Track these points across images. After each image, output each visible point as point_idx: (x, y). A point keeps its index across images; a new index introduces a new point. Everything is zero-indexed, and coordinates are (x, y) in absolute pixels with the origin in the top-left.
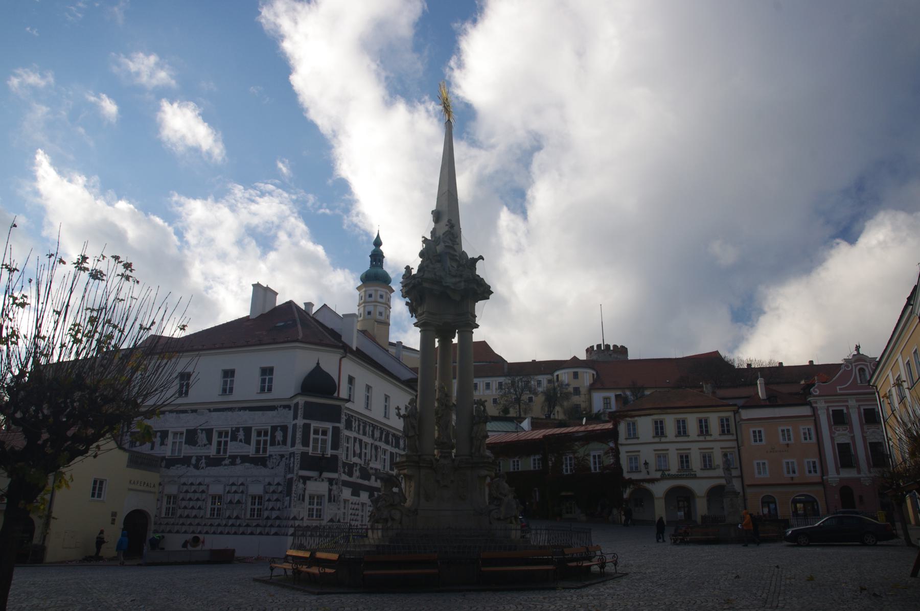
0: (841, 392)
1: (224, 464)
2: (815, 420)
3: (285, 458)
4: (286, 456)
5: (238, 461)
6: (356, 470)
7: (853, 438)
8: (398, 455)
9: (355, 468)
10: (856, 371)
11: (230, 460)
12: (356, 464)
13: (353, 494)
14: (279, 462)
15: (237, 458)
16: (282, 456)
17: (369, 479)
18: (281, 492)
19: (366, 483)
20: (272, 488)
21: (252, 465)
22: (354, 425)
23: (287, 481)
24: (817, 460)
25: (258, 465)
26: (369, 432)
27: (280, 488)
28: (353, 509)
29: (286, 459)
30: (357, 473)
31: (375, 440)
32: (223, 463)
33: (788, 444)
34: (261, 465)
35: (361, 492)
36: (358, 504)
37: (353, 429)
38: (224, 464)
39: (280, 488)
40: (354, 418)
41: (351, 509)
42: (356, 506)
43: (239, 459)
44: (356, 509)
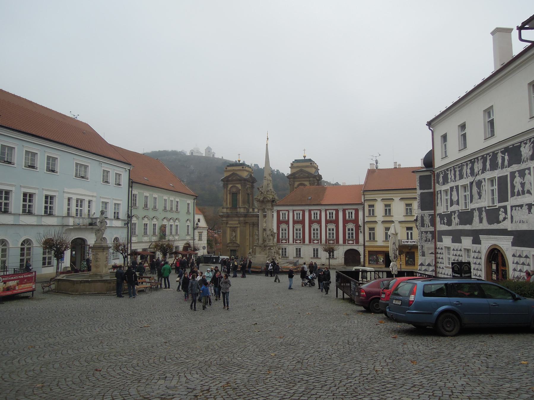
6: (454, 218)
8: (517, 174)
9: (453, 216)
12: (454, 212)
13: (454, 241)
17: (470, 222)
19: (468, 227)
22: (449, 176)
26: (467, 172)
28: (456, 255)
30: (456, 220)
31: (476, 176)
35: (462, 238)
36: (461, 250)
37: (449, 180)
40: (449, 169)
41: (453, 255)
42: (459, 253)
44: (459, 256)
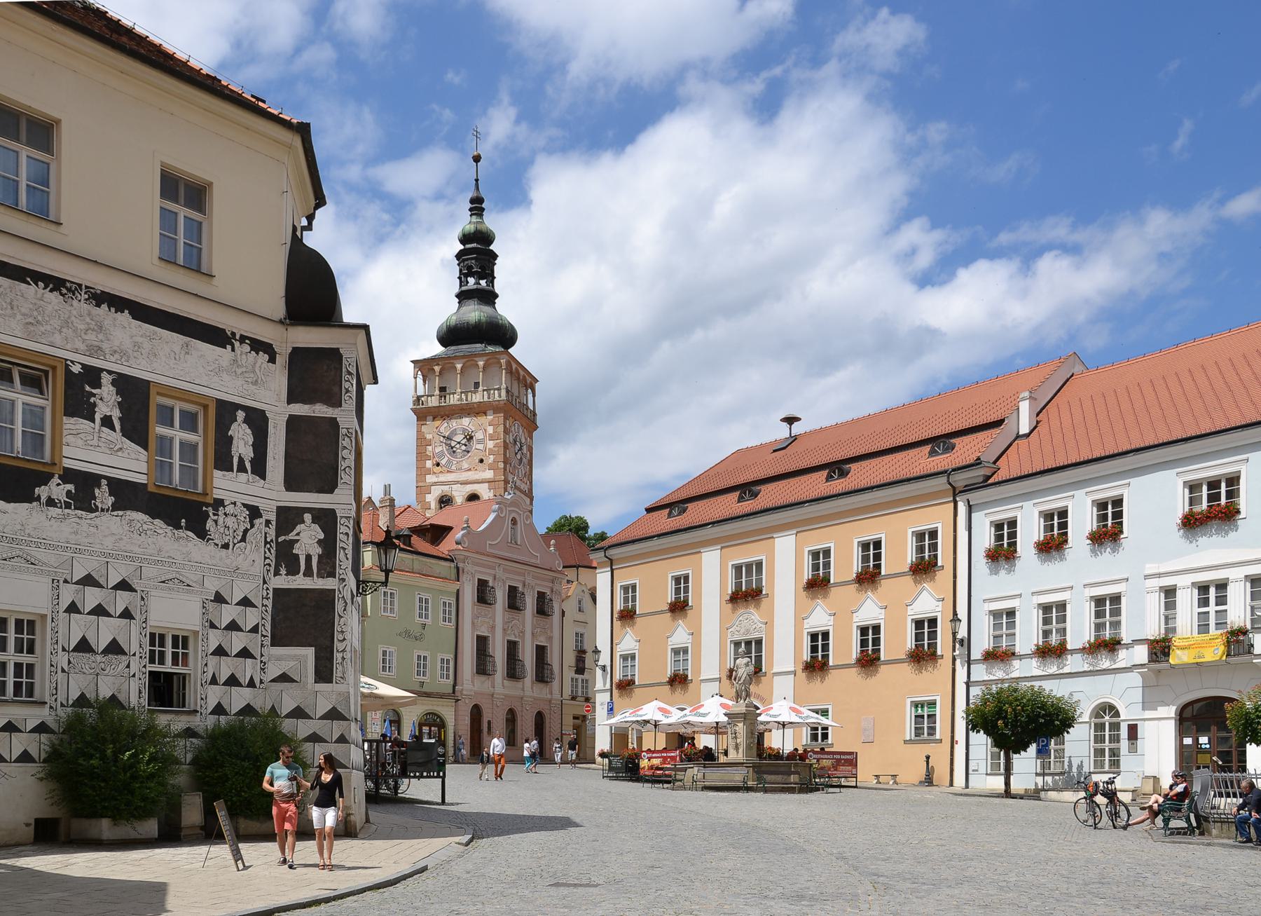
0: (492, 551)
1: (44, 498)
2: (458, 590)
3: (262, 520)
4: (265, 517)
5: (103, 497)
7: (493, 628)
10: (508, 523)
11: (70, 487)
14: (246, 531)
15: (99, 486)
16: (254, 512)
18: (255, 630)
20: (228, 613)
21: (157, 521)
23: (271, 595)
24: (451, 657)
25: (178, 527)
27: (251, 617)
29: (268, 522)
32: (42, 492)
33: (424, 626)
34: (187, 529)
38: (44, 498)
39: (251, 617)
43: (105, 488)
